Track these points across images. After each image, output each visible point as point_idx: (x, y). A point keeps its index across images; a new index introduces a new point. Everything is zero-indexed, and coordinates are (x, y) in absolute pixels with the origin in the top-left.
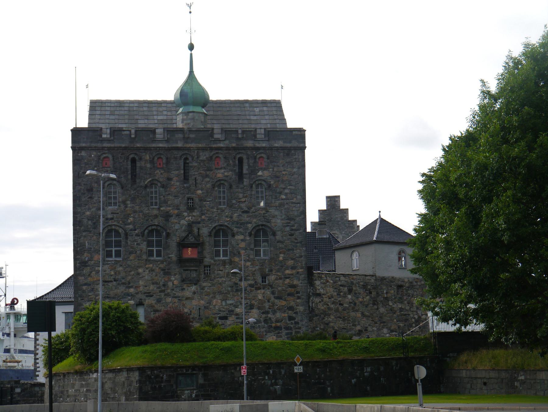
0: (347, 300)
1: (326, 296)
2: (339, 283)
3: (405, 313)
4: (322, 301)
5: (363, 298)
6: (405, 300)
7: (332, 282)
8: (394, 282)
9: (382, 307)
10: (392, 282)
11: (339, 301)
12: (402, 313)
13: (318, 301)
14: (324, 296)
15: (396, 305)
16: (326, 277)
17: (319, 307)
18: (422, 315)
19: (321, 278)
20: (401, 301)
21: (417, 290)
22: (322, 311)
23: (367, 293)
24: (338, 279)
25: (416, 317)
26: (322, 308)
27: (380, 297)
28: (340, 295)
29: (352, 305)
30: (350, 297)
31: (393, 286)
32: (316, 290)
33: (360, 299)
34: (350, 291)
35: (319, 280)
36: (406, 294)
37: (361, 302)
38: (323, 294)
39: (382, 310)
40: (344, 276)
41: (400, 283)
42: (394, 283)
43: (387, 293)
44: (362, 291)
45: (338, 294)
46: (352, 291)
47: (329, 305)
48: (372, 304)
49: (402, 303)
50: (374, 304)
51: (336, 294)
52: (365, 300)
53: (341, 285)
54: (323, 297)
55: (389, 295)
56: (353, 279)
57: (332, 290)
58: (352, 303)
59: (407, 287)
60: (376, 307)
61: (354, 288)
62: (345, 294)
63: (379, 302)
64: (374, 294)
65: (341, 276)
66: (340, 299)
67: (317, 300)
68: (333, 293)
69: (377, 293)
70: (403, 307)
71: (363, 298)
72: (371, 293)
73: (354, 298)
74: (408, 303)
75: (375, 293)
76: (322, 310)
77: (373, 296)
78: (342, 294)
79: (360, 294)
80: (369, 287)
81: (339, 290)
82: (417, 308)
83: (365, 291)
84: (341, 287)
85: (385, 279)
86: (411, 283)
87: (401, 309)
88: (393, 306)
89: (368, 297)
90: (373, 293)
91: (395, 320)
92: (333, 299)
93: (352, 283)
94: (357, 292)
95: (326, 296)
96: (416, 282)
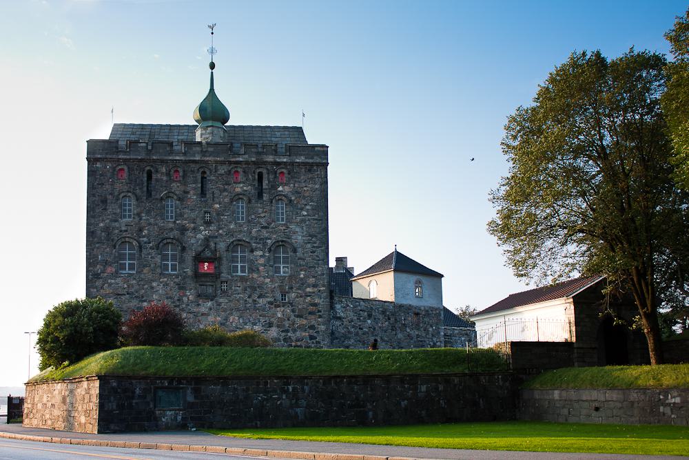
2: (359, 308)
4: (343, 324)
11: (360, 325)
20: (417, 327)
26: (343, 331)
28: (359, 319)
30: (369, 321)
34: (370, 316)
37: (380, 327)
39: (400, 336)
41: (417, 311)
44: (381, 317)
51: (355, 318)
57: (352, 314)
60: (394, 332)
61: (373, 314)
64: (392, 320)
67: (338, 323)
69: (396, 320)
72: (389, 319)
78: (361, 318)
81: (359, 314)
82: (433, 335)
86: (427, 311)
87: (418, 336)
89: (387, 323)
93: (372, 308)
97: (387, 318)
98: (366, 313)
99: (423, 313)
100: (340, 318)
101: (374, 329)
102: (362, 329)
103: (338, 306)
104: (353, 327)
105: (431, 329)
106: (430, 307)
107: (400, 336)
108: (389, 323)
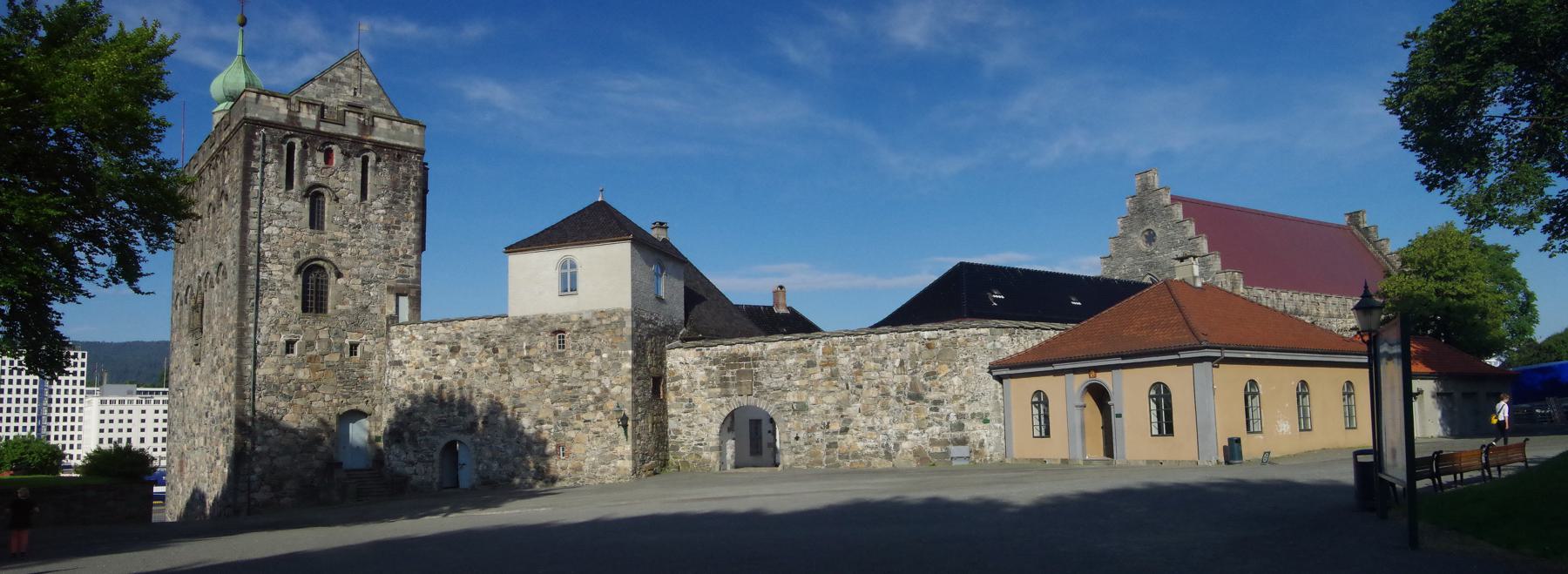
0: (448, 369)
1: (411, 365)
2: (435, 339)
3: (570, 385)
4: (404, 373)
5: (480, 362)
6: (573, 358)
7: (421, 338)
8: (546, 324)
9: (521, 375)
10: (541, 324)
11: (435, 371)
12: (565, 384)
13: (398, 374)
14: (407, 365)
15: (549, 370)
16: (411, 331)
17: (398, 385)
18: (613, 386)
19: (402, 333)
20: (561, 358)
21: (599, 336)
22: (401, 392)
23: (488, 352)
24: (432, 331)
25: (597, 391)
26: (404, 386)
27: (514, 356)
28: (435, 360)
29: (460, 376)
30: (453, 362)
31: (542, 333)
32: (393, 356)
33: (475, 365)
34: (454, 350)
35: (398, 337)
36: (573, 348)
37: (477, 371)
38: (405, 362)
39: (519, 381)
40: (444, 326)
41: (557, 326)
42: (546, 327)
43: (528, 348)
44: (478, 349)
45: (431, 360)
46: (457, 352)
47: (417, 379)
48: (499, 372)
49: (564, 364)
50: (503, 372)
51: (427, 359)
52: (484, 365)
53: (437, 343)
54: (405, 368)
55: (532, 353)
56: (461, 328)
57: (420, 352)
58: (458, 372)
59: (575, 332)
60: (506, 377)
61: (462, 346)
62: (445, 357)
63: (514, 368)
64: (502, 352)
65: (437, 325)
66: (434, 368)
67: (396, 372)
68: (422, 357)
69: (509, 350)
70: (565, 373)
71: (480, 362)
72: (495, 351)
73: (461, 364)
74: (579, 364)
75: (505, 351)
76: (404, 390)
77: (500, 357)
78: (439, 358)
79: (473, 354)
80: (493, 340)
81: (434, 351)
82: (601, 373)
83: (485, 347)
84: (438, 346)
85: (527, 321)
86: (587, 322)
87: (562, 379)
88: (543, 373)
89: (490, 360)
90: (499, 350)
91: (548, 400)
92: (423, 369)
93: (459, 336)
94: (468, 351)
95: (411, 365)
96: (598, 319)
97: (490, 349)
98: (446, 348)
99: (575, 328)
100: (399, 363)
101: (465, 375)
102: (440, 378)
103: (396, 342)
104: (424, 375)
105: (596, 360)
106: (595, 313)
107: (519, 381)
108: (496, 359)
